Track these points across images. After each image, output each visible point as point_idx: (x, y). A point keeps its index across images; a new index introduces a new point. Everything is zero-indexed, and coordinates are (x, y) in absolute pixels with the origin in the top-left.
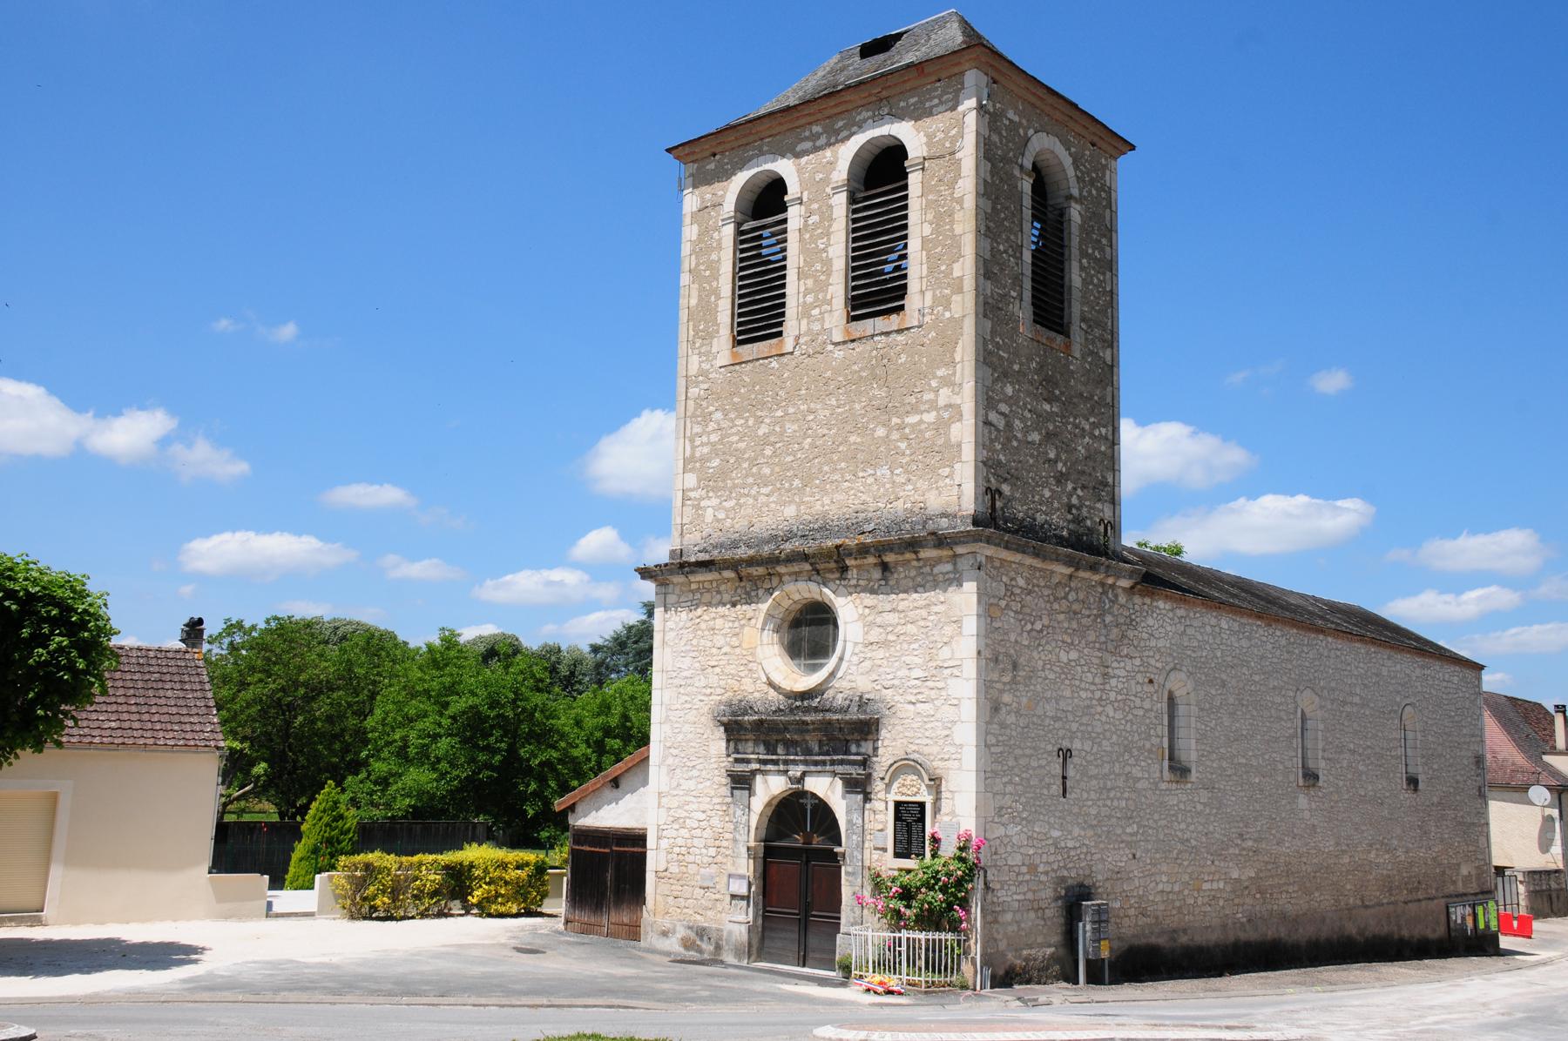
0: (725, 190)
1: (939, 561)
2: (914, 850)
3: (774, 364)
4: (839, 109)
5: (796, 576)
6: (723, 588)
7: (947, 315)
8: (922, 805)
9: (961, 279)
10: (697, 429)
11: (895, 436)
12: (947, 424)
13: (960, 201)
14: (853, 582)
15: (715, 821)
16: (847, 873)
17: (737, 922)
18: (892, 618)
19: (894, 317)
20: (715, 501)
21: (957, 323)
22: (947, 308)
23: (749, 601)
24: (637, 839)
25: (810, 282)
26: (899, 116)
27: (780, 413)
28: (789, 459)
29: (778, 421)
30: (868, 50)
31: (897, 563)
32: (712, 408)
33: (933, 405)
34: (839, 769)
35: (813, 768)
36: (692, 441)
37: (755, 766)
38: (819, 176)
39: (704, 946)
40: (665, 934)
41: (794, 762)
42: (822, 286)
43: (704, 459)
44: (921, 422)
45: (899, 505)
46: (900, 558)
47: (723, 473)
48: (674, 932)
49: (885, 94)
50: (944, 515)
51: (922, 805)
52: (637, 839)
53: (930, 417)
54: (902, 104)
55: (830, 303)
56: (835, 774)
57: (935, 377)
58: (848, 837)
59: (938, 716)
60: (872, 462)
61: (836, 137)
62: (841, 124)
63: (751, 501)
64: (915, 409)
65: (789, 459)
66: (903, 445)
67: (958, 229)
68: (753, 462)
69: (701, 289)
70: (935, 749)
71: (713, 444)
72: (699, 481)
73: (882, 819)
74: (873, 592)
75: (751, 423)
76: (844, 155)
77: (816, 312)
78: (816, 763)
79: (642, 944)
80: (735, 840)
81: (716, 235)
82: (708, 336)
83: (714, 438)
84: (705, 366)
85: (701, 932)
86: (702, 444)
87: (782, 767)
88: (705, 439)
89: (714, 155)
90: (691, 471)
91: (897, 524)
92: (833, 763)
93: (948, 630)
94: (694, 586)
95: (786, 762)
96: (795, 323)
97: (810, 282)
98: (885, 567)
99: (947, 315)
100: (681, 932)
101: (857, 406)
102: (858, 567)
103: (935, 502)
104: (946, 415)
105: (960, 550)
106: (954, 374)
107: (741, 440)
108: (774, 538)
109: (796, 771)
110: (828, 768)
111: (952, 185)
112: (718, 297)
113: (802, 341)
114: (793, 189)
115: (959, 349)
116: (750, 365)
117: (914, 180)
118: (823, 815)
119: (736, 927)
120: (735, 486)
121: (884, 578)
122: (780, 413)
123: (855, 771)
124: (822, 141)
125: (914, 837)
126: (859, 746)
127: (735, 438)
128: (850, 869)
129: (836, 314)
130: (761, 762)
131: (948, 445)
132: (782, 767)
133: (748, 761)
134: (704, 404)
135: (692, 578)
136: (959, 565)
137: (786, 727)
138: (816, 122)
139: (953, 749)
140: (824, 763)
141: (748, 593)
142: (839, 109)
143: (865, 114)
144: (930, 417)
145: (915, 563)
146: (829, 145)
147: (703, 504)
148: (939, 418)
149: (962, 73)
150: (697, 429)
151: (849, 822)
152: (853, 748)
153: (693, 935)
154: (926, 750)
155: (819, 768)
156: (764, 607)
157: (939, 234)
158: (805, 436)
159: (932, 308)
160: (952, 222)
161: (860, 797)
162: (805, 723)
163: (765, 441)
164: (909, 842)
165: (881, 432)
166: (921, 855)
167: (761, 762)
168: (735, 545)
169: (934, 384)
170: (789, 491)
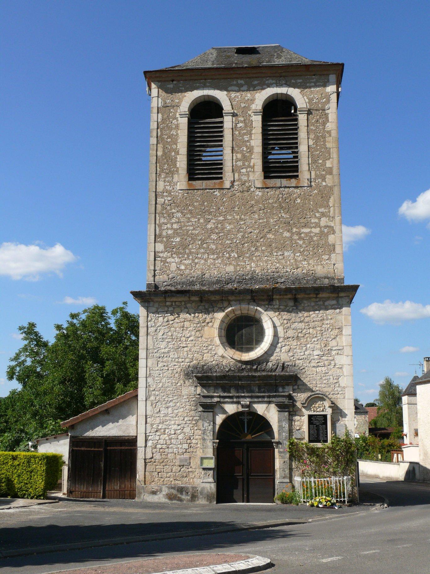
0: (181, 100)
1: (328, 298)
2: (321, 439)
3: (217, 193)
4: (257, 75)
5: (240, 301)
6: (189, 305)
7: (324, 184)
8: (325, 416)
9: (331, 168)
10: (162, 220)
11: (296, 237)
12: (327, 235)
13: (329, 132)
14: (277, 306)
15: (187, 430)
16: (279, 452)
17: (207, 483)
18: (302, 325)
19: (293, 180)
20: (177, 260)
21: (331, 188)
22: (324, 179)
23: (207, 312)
24: (132, 442)
25: (239, 156)
26: (290, 86)
27: (221, 218)
28: (229, 242)
29: (221, 222)
30: (240, 51)
31: (303, 299)
32: (173, 210)
33: (317, 225)
34: (274, 399)
35: (256, 400)
36: (160, 226)
37: (216, 400)
38: (243, 105)
39: (183, 497)
40: (154, 493)
41: (244, 397)
42: (245, 159)
43: (168, 237)
44: (311, 232)
45: (299, 270)
46: (307, 296)
47: (184, 246)
48: (161, 491)
49: (284, 74)
50: (325, 278)
51: (325, 416)
52: (132, 442)
53: (317, 230)
54: (293, 81)
55: (253, 167)
56: (269, 403)
57: (318, 212)
58: (279, 434)
59: (330, 373)
60: (283, 248)
61: (252, 88)
62: (256, 82)
63: (203, 262)
64: (305, 226)
65: (229, 242)
66: (301, 242)
67: (328, 145)
68: (203, 241)
69: (164, 148)
70: (330, 389)
71: (176, 230)
72: (165, 248)
73: (302, 424)
74: (288, 311)
75: (202, 221)
76: (261, 97)
77: (244, 170)
78: (258, 397)
79: (137, 499)
80: (204, 439)
81: (174, 121)
82: (171, 173)
83: (175, 226)
84: (168, 188)
85: (181, 490)
86: (167, 229)
87: (235, 400)
88: (169, 226)
89: (173, 81)
90: (161, 242)
91: (297, 279)
92: (269, 397)
93: (336, 332)
94: (168, 304)
95: (238, 397)
96: (231, 174)
97: (239, 156)
98: (296, 300)
99: (324, 184)
100: (165, 491)
101: (272, 221)
102: (280, 300)
103: (320, 271)
104: (326, 231)
105: (342, 294)
106: (329, 212)
107: (194, 229)
108: (218, 282)
109: (246, 401)
110: (266, 399)
111: (324, 124)
112: (177, 153)
113: (236, 184)
114: (226, 106)
115: (331, 200)
116: (200, 192)
117: (302, 119)
118: (262, 424)
119: (208, 485)
120: (191, 253)
121: (295, 305)
122: (221, 218)
123: (286, 401)
124: (245, 88)
125: (321, 432)
126: (284, 388)
127: (192, 228)
128: (281, 450)
129: (258, 174)
130: (220, 397)
131: (327, 244)
132: (235, 400)
133: (212, 397)
134: (168, 208)
135: (168, 299)
136: (340, 302)
137: (240, 378)
138: (241, 78)
139: (339, 389)
140: (263, 397)
141: (205, 309)
142: (257, 75)
143: (270, 81)
144: (317, 230)
145: (314, 300)
146: (248, 90)
147: (168, 260)
148: (322, 232)
149: (328, 75)
150: (162, 220)
151: (280, 427)
152: (280, 389)
153: (174, 492)
154: (325, 390)
155: (260, 400)
156: (220, 315)
157: (317, 145)
158: (238, 231)
159: (315, 179)
160: (325, 141)
161: (286, 414)
162: (255, 377)
163: (212, 231)
164: (318, 434)
165: (287, 234)
166: (326, 441)
167: (220, 397)
168: (192, 283)
169: (317, 215)
170: (229, 258)
